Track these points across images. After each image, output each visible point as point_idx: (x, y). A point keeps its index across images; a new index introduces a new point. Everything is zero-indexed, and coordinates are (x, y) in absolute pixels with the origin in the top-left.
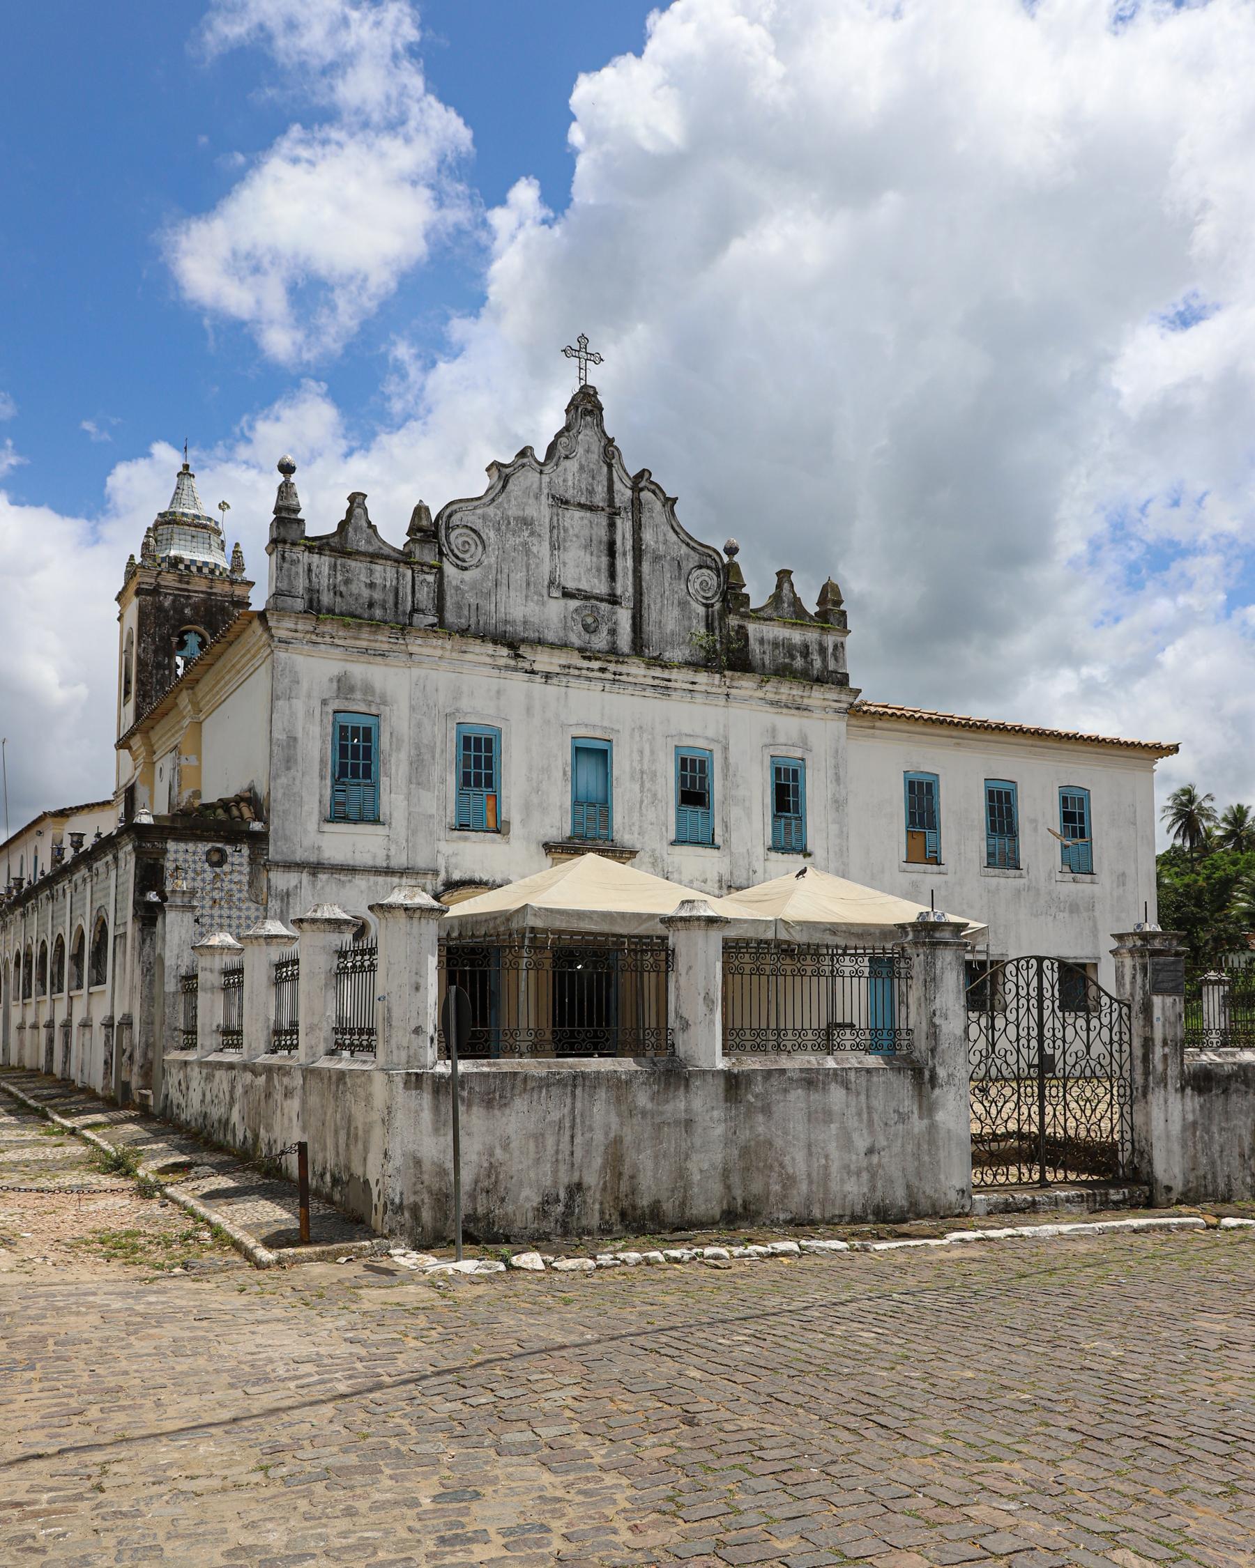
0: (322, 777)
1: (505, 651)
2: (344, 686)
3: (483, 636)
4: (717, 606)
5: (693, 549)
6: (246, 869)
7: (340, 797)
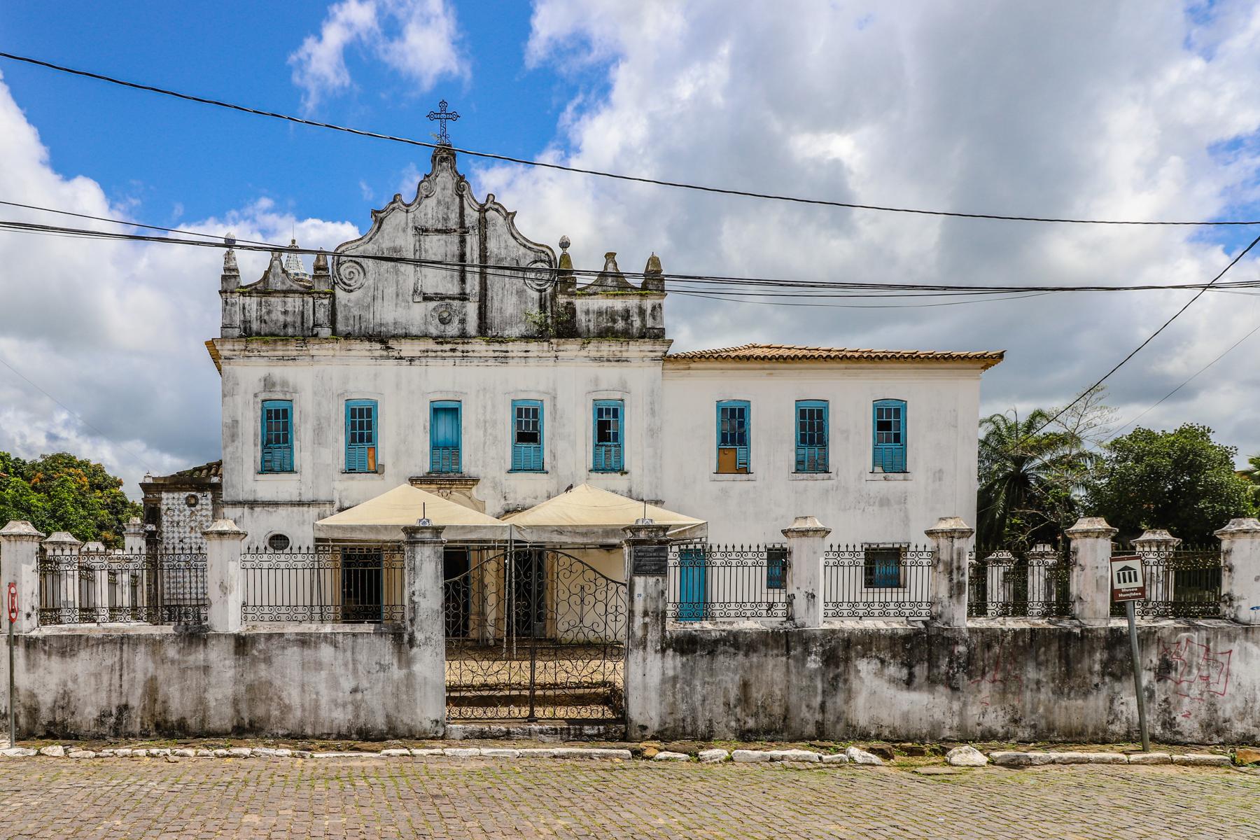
0: (255, 445)
1: (378, 346)
2: (268, 384)
3: (370, 337)
4: (549, 290)
5: (530, 248)
6: (210, 507)
7: (268, 457)
